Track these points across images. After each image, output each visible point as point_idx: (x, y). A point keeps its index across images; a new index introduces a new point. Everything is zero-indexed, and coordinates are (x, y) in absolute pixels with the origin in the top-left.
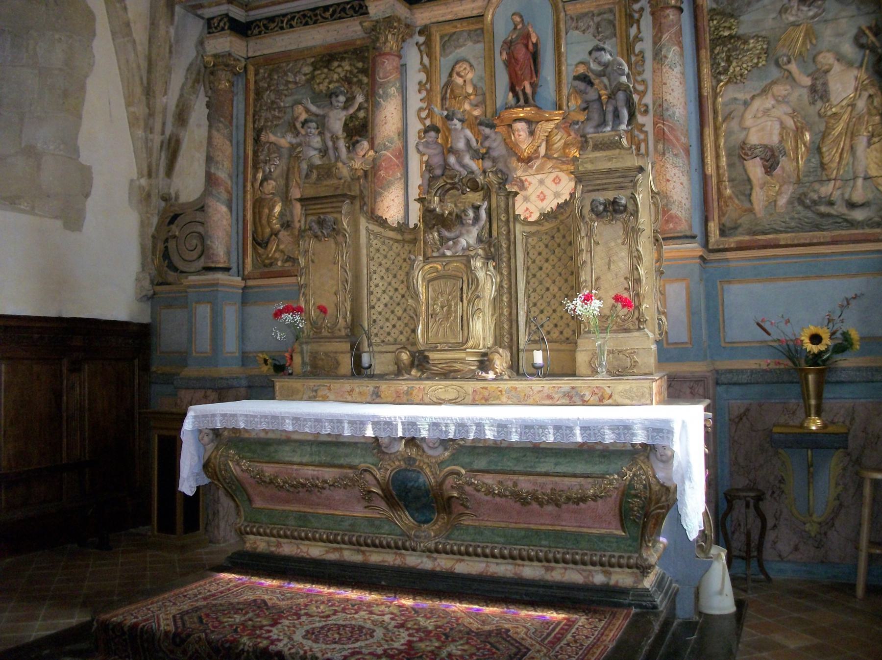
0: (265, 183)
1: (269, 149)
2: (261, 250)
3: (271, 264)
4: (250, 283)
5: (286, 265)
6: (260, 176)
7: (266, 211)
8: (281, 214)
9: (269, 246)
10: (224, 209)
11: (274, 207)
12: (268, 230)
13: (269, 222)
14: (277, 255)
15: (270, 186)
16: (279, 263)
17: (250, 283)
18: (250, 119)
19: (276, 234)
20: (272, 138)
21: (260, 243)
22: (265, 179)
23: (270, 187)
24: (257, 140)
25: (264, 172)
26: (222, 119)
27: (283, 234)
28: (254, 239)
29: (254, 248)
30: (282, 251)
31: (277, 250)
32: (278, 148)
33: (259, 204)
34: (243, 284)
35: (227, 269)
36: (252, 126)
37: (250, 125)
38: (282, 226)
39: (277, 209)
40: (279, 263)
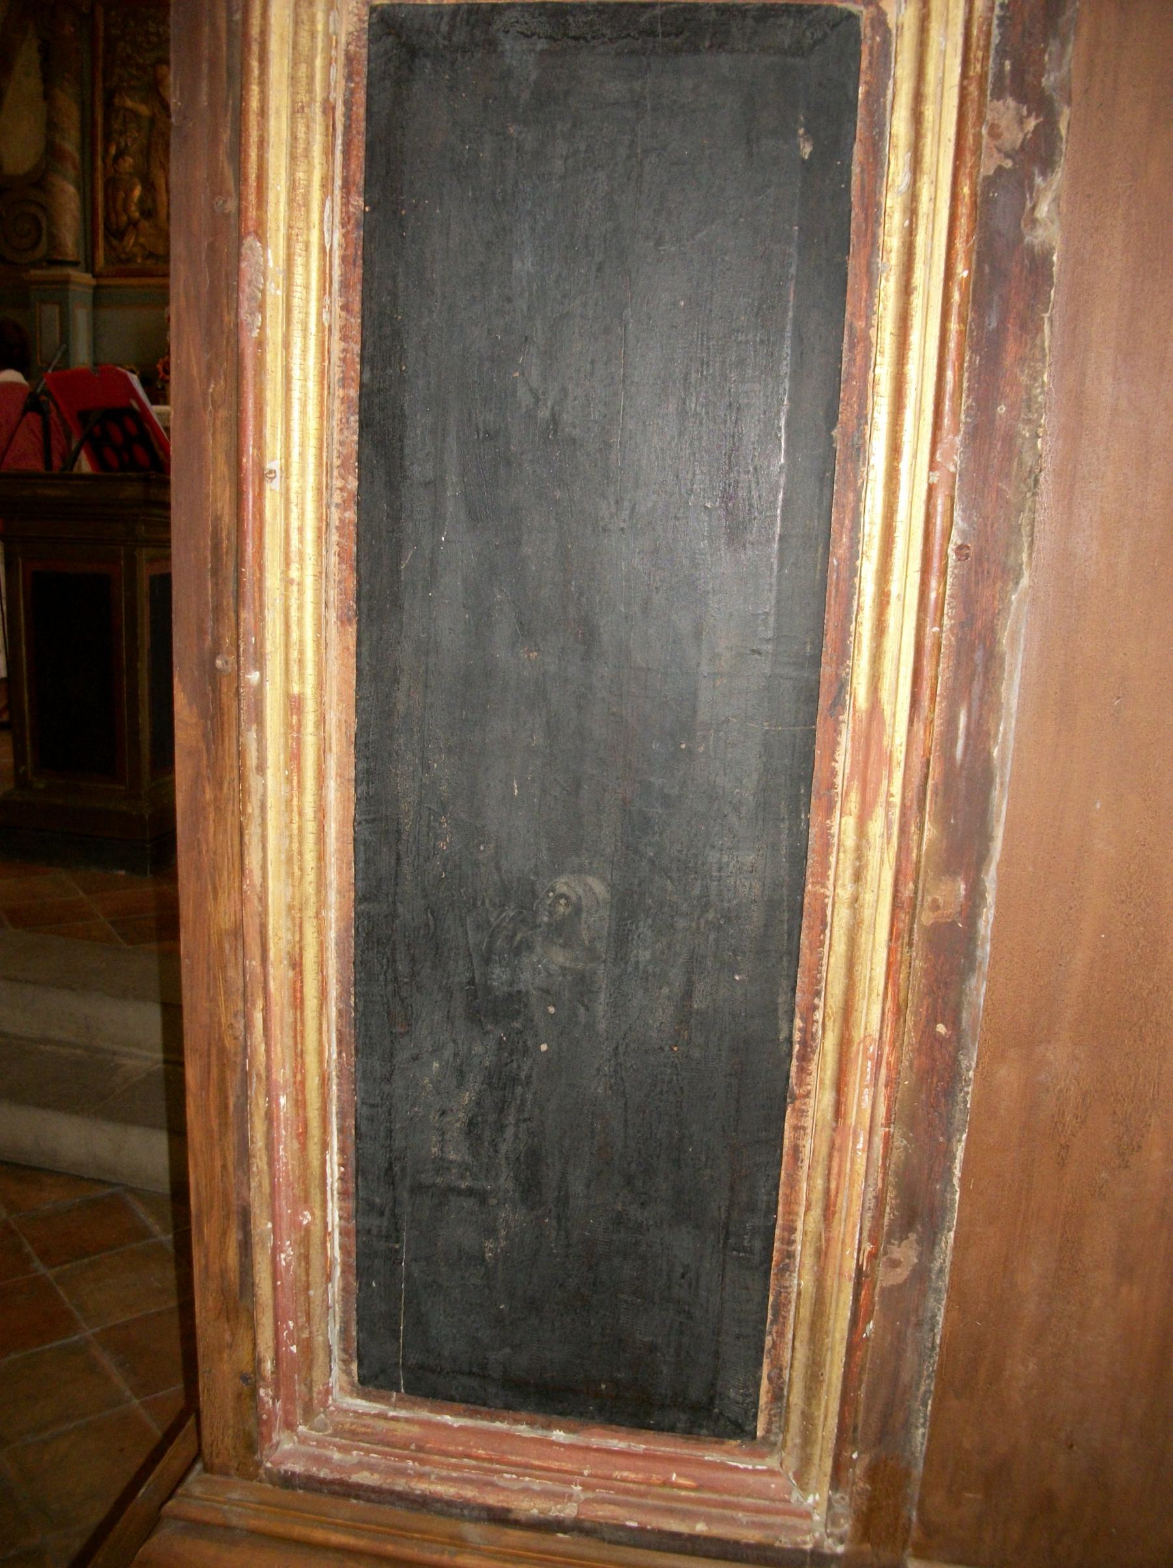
0: (121, 160)
1: (124, 116)
2: (115, 242)
3: (128, 261)
4: (104, 282)
5: (148, 262)
6: (113, 150)
7: (122, 195)
8: (141, 200)
9: (126, 238)
10: (71, 189)
11: (132, 190)
12: (124, 218)
13: (126, 210)
14: (136, 250)
15: (128, 163)
16: (139, 260)
17: (104, 282)
18: (99, 76)
19: (134, 224)
20: (129, 103)
21: (115, 233)
22: (120, 154)
23: (127, 165)
24: (109, 105)
25: (118, 144)
26: (66, 75)
27: (145, 225)
28: (106, 227)
29: (106, 238)
30: (143, 246)
31: (136, 243)
32: (136, 115)
33: (112, 184)
34: (93, 282)
35: (75, 264)
36: (101, 84)
37: (100, 85)
38: (142, 213)
39: (137, 192)
40: (139, 260)
